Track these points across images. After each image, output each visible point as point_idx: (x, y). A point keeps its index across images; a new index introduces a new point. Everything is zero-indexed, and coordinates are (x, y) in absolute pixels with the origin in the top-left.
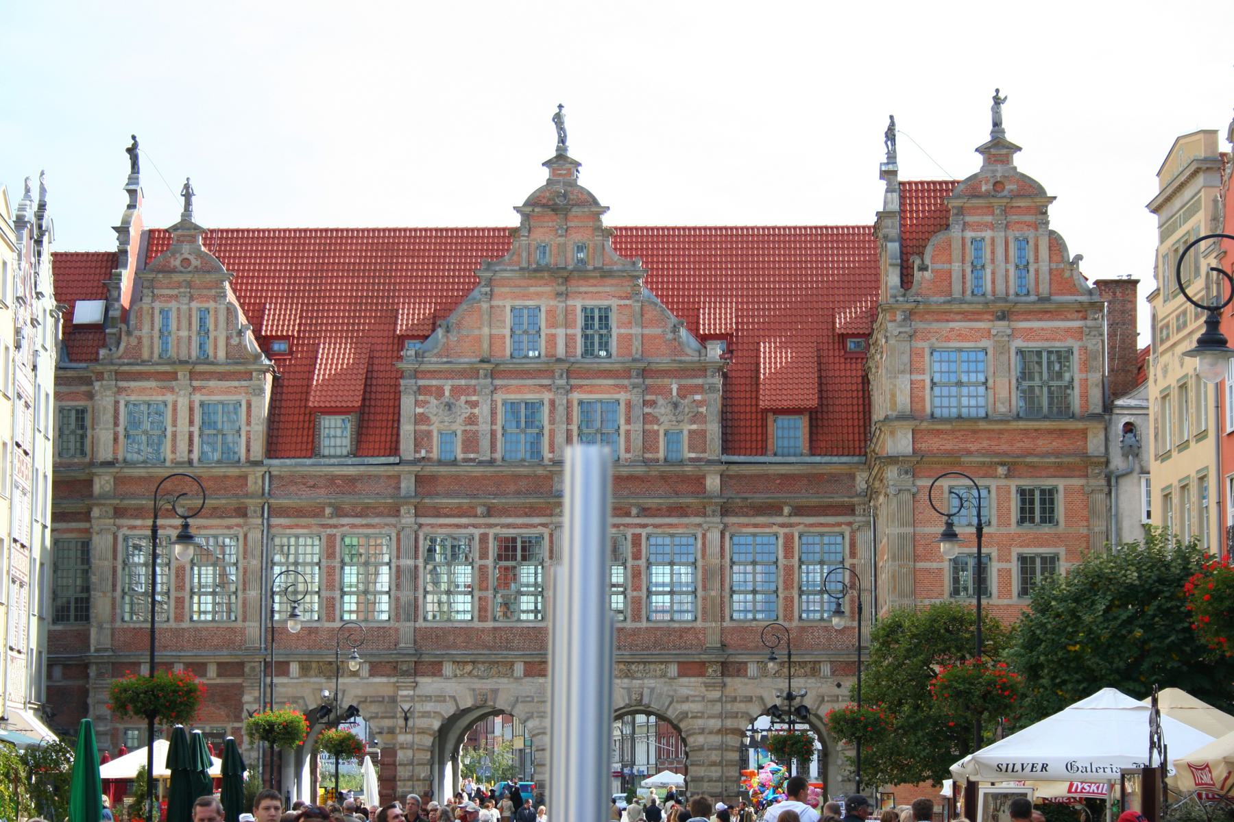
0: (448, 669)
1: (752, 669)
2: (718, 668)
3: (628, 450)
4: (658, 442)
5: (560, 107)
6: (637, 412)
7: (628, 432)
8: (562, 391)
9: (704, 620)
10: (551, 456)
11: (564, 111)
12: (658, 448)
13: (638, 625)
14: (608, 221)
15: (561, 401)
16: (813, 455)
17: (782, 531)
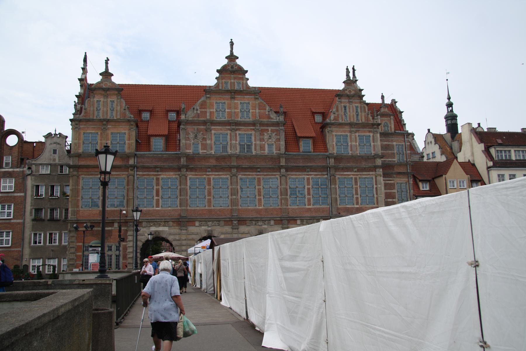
0: (197, 224)
1: (299, 222)
2: (286, 222)
3: (255, 150)
4: (265, 147)
5: (231, 40)
6: (258, 138)
7: (255, 144)
8: (234, 130)
9: (281, 206)
10: (230, 151)
11: (232, 41)
12: (265, 149)
13: (261, 208)
14: (247, 75)
15: (233, 134)
16: (314, 152)
17: (306, 177)
